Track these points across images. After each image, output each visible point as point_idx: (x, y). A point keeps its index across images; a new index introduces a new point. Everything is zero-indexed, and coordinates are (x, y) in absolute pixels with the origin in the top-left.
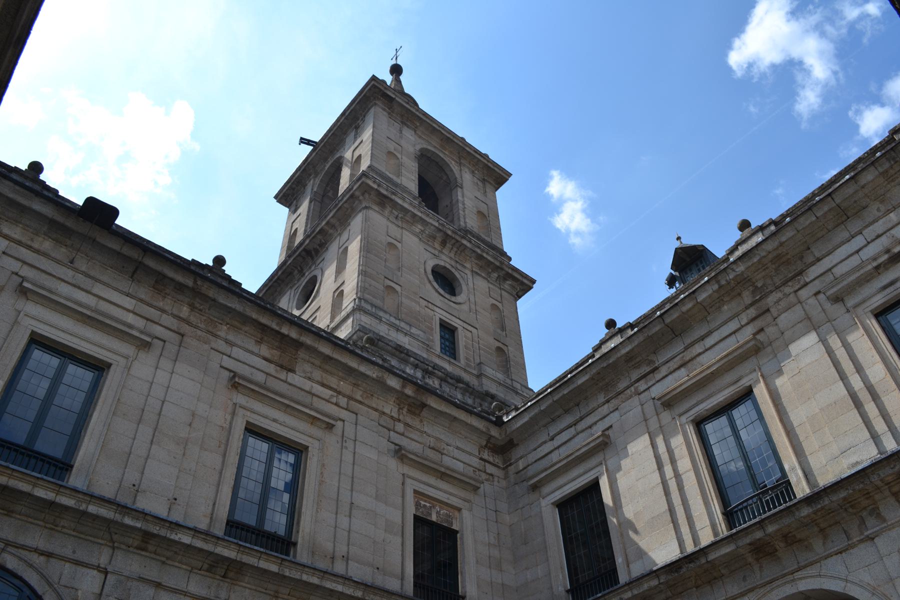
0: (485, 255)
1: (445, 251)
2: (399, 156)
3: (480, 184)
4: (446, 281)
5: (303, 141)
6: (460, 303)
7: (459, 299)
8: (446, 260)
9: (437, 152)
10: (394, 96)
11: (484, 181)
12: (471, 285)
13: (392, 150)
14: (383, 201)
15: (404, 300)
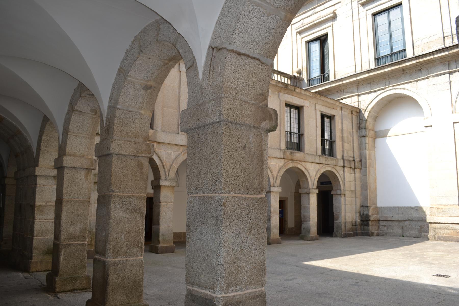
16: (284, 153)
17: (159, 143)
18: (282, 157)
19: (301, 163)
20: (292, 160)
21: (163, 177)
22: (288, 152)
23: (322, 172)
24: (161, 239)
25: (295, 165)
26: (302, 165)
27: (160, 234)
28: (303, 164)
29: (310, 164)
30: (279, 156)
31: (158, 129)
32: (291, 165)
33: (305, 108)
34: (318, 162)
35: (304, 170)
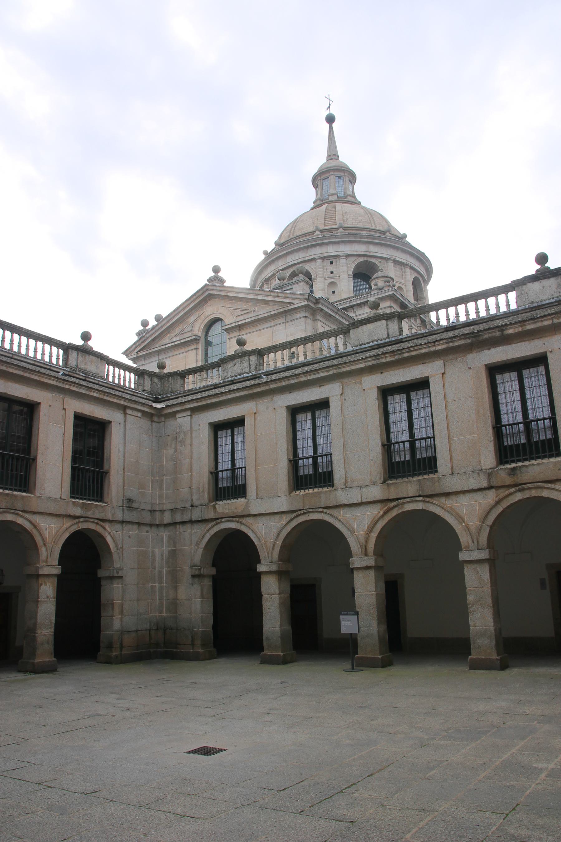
16: (490, 475)
17: (255, 515)
18: (485, 484)
19: (549, 485)
20: (519, 486)
21: (263, 561)
24: (265, 644)
25: (534, 493)
27: (264, 638)
30: (475, 486)
31: (251, 498)
32: (519, 496)
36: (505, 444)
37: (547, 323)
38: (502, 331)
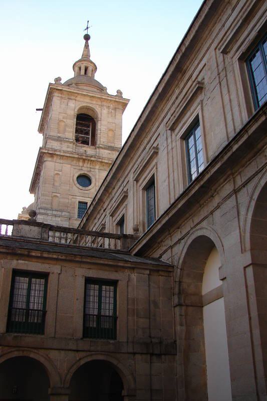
0: (103, 161)
1: (85, 165)
2: (65, 120)
3: (113, 111)
4: (84, 180)
5: (37, 110)
6: (90, 189)
7: (90, 187)
8: (85, 171)
9: (88, 105)
10: (61, 88)
11: (115, 109)
12: (97, 177)
13: (62, 119)
14: (52, 155)
15: (62, 200)
19: (36, 351)
22: (10, 337)
23: (82, 362)
25: (25, 354)
26: (38, 354)
28: (42, 352)
29: (57, 352)
32: (16, 354)
33: (50, 274)
34: (74, 348)
35: (42, 360)
36: (29, 321)
37: (55, 256)
38: (29, 252)
